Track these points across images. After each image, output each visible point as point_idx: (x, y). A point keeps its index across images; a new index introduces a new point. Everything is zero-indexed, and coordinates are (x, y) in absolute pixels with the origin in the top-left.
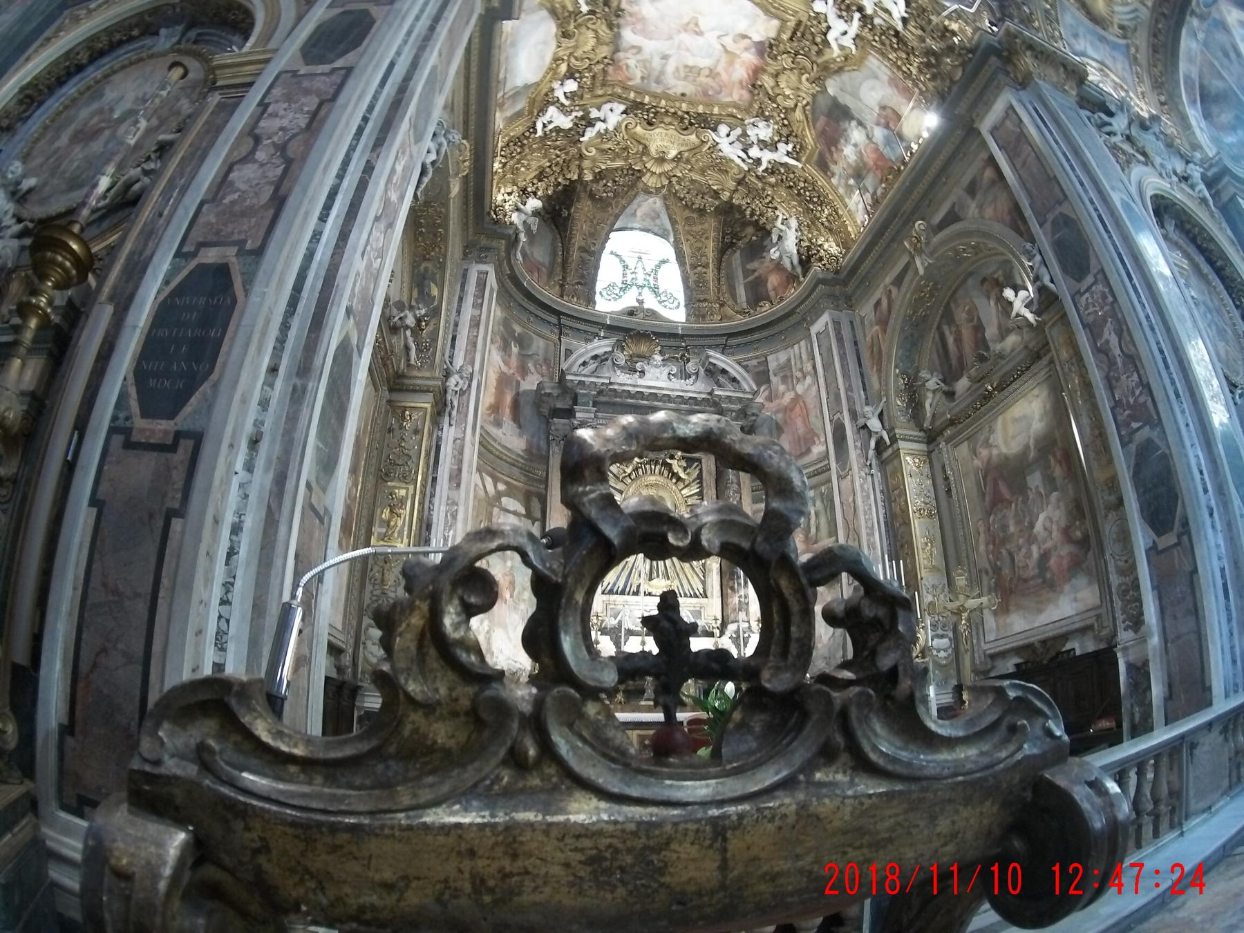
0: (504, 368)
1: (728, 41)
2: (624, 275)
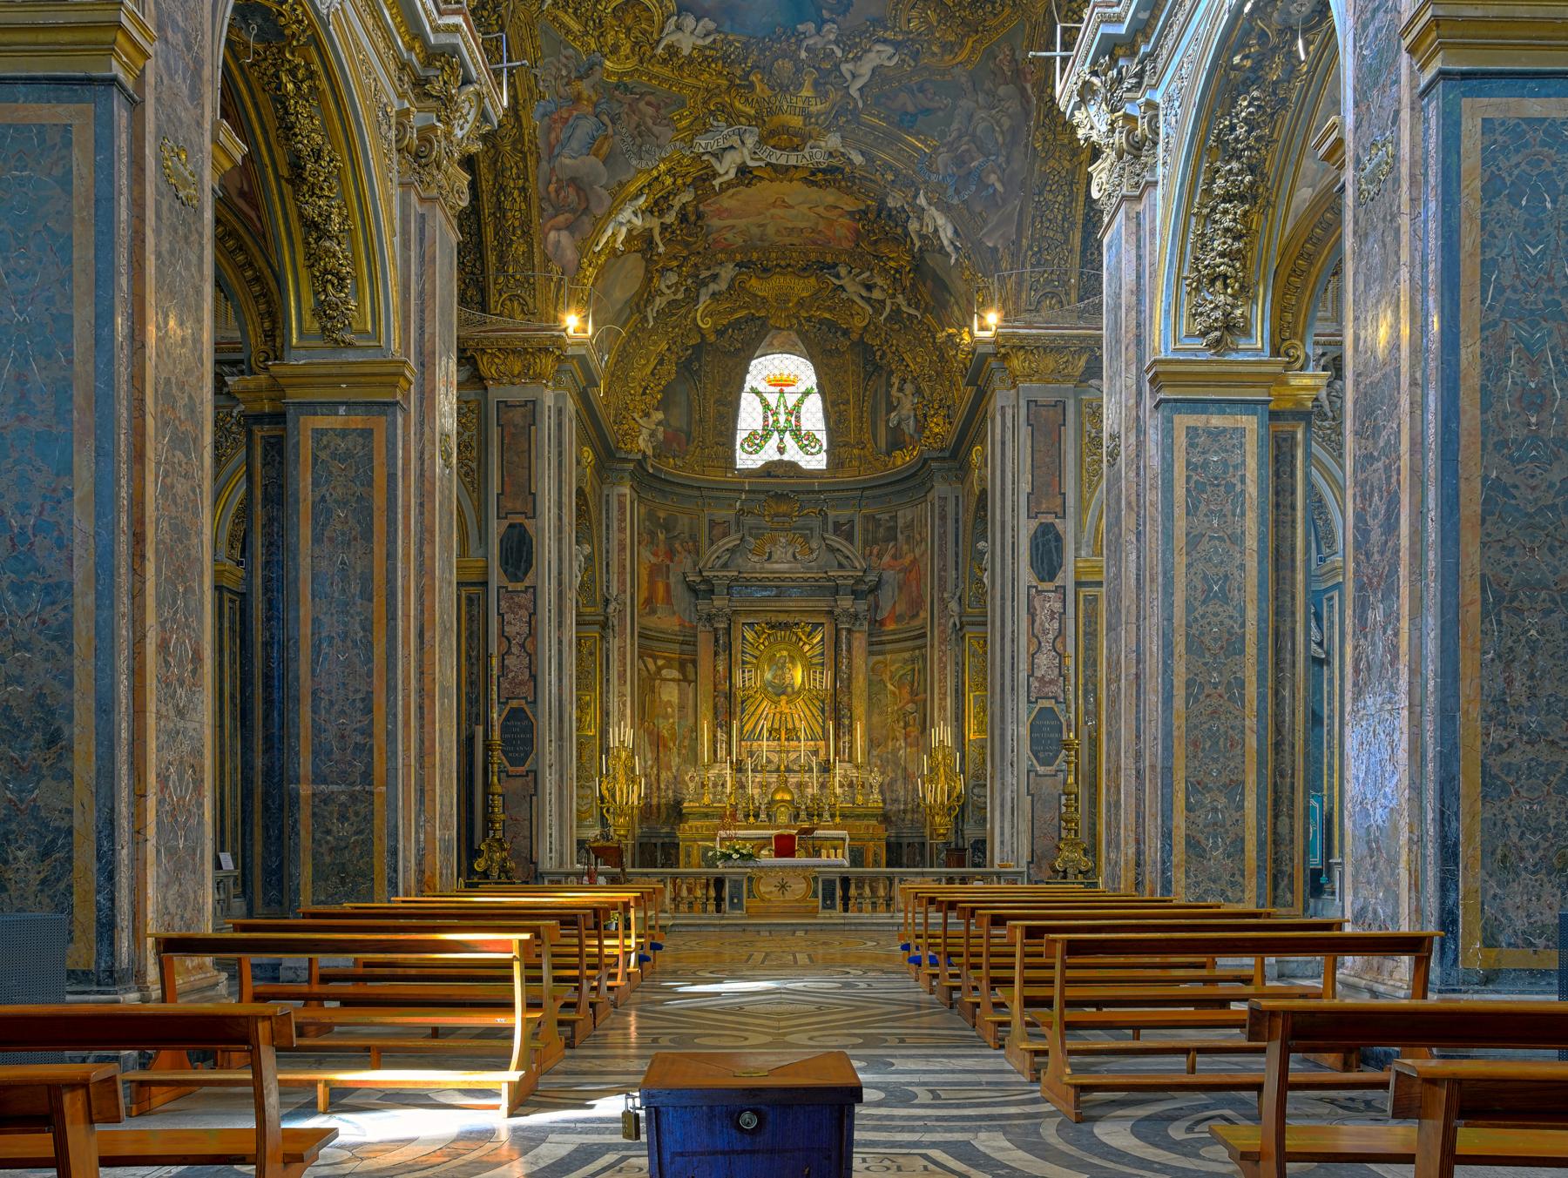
0: (653, 560)
1: (821, 210)
2: (765, 418)
